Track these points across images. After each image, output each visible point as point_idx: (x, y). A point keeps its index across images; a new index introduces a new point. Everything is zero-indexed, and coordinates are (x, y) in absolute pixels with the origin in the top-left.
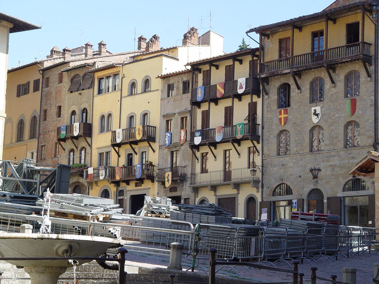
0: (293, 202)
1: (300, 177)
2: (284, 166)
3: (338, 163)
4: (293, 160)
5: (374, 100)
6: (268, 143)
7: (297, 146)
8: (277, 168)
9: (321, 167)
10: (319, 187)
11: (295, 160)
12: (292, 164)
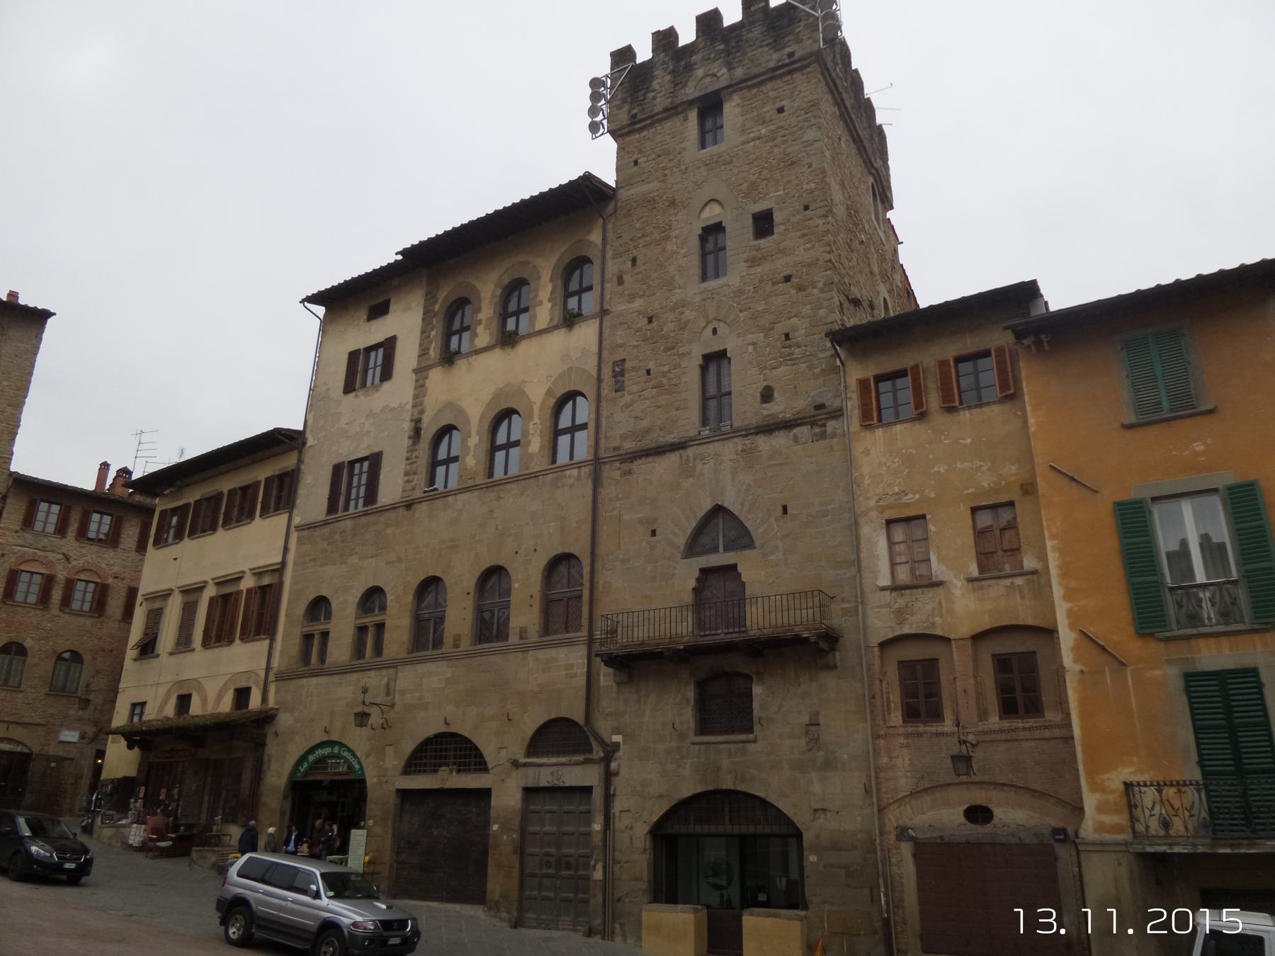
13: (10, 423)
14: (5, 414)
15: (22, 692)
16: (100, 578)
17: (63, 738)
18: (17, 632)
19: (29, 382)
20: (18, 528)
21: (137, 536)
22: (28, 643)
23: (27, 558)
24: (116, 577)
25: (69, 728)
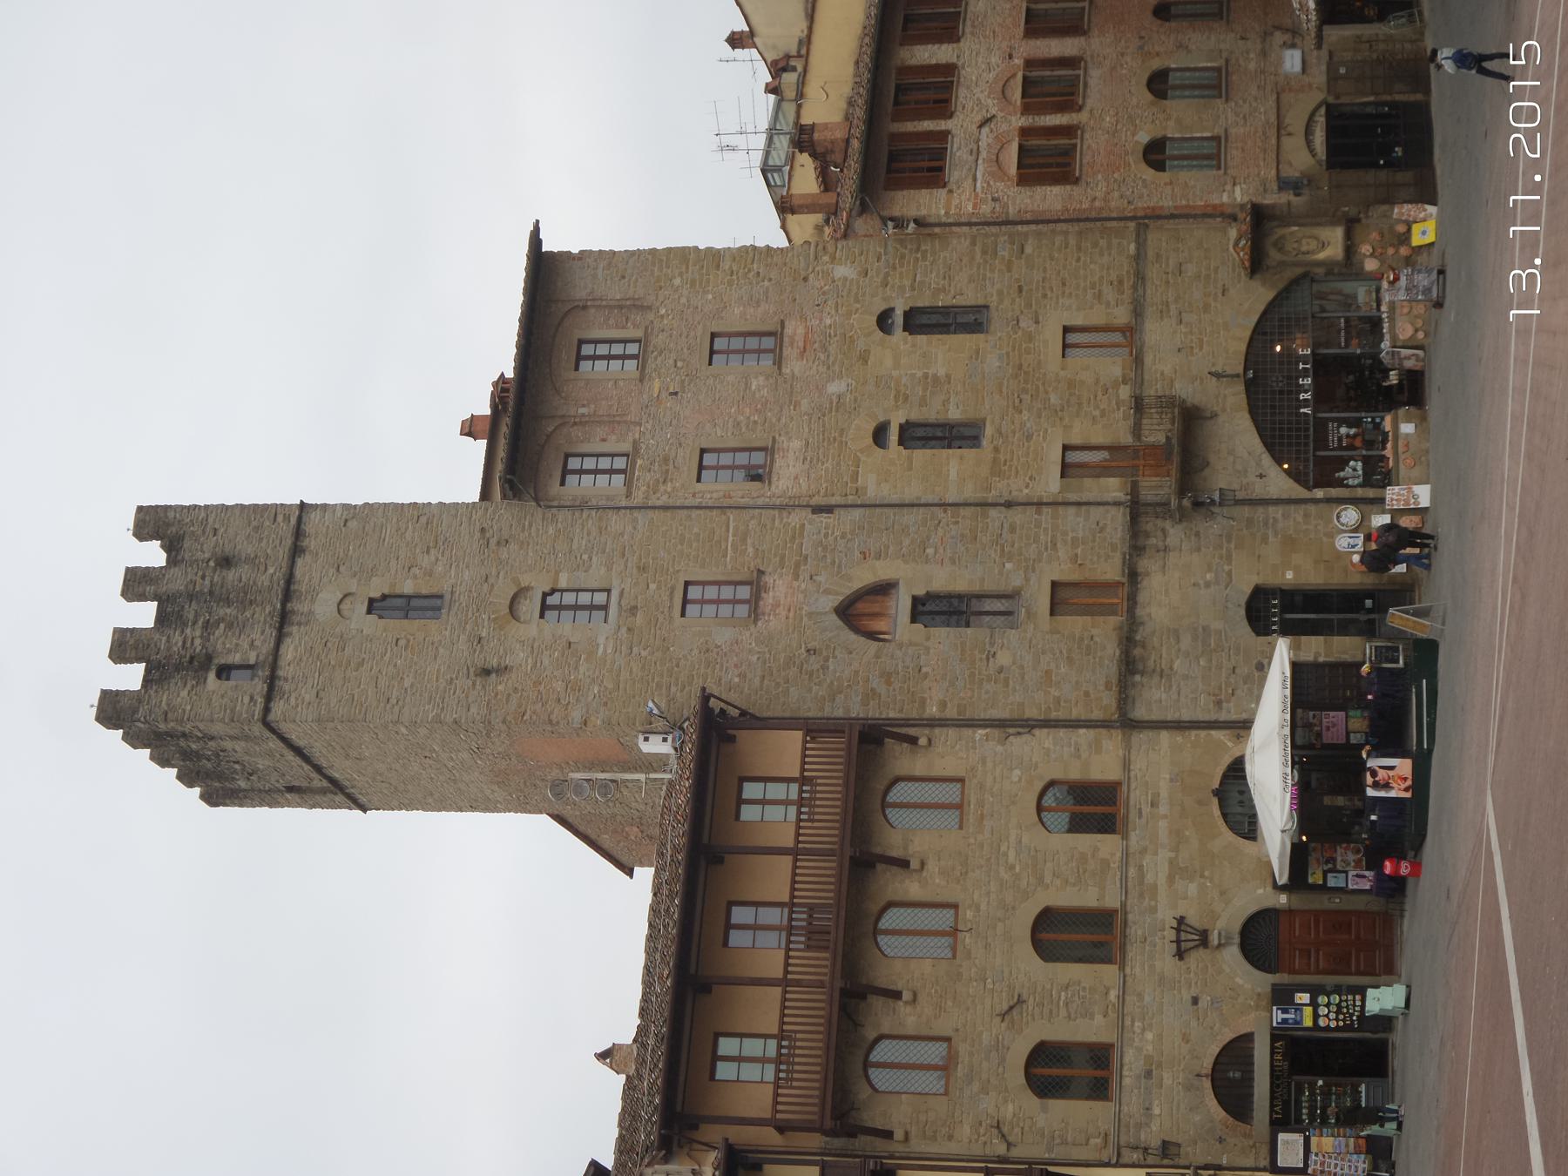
0: (1279, 1020)
1: (1195, 1001)
2: (1152, 1071)
3: (1165, 855)
4: (1136, 1029)
5: (988, 730)
6: (1064, 1142)
7: (1092, 1017)
8: (1157, 1102)
9: (1167, 916)
10: (1237, 926)
11: (1137, 1024)
12: (1149, 1036)
13: (749, 261)
14: (734, 269)
15: (1226, 130)
16: (1014, 76)
17: (1298, 67)
18: (1127, 153)
19: (669, 250)
20: (942, 193)
21: (930, 46)
22: (1144, 138)
23: (995, 168)
24: (1011, 57)
25: (1280, 62)
